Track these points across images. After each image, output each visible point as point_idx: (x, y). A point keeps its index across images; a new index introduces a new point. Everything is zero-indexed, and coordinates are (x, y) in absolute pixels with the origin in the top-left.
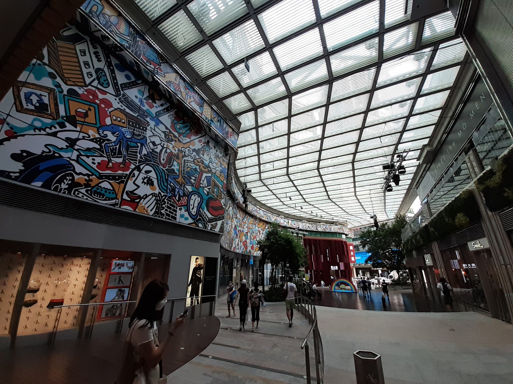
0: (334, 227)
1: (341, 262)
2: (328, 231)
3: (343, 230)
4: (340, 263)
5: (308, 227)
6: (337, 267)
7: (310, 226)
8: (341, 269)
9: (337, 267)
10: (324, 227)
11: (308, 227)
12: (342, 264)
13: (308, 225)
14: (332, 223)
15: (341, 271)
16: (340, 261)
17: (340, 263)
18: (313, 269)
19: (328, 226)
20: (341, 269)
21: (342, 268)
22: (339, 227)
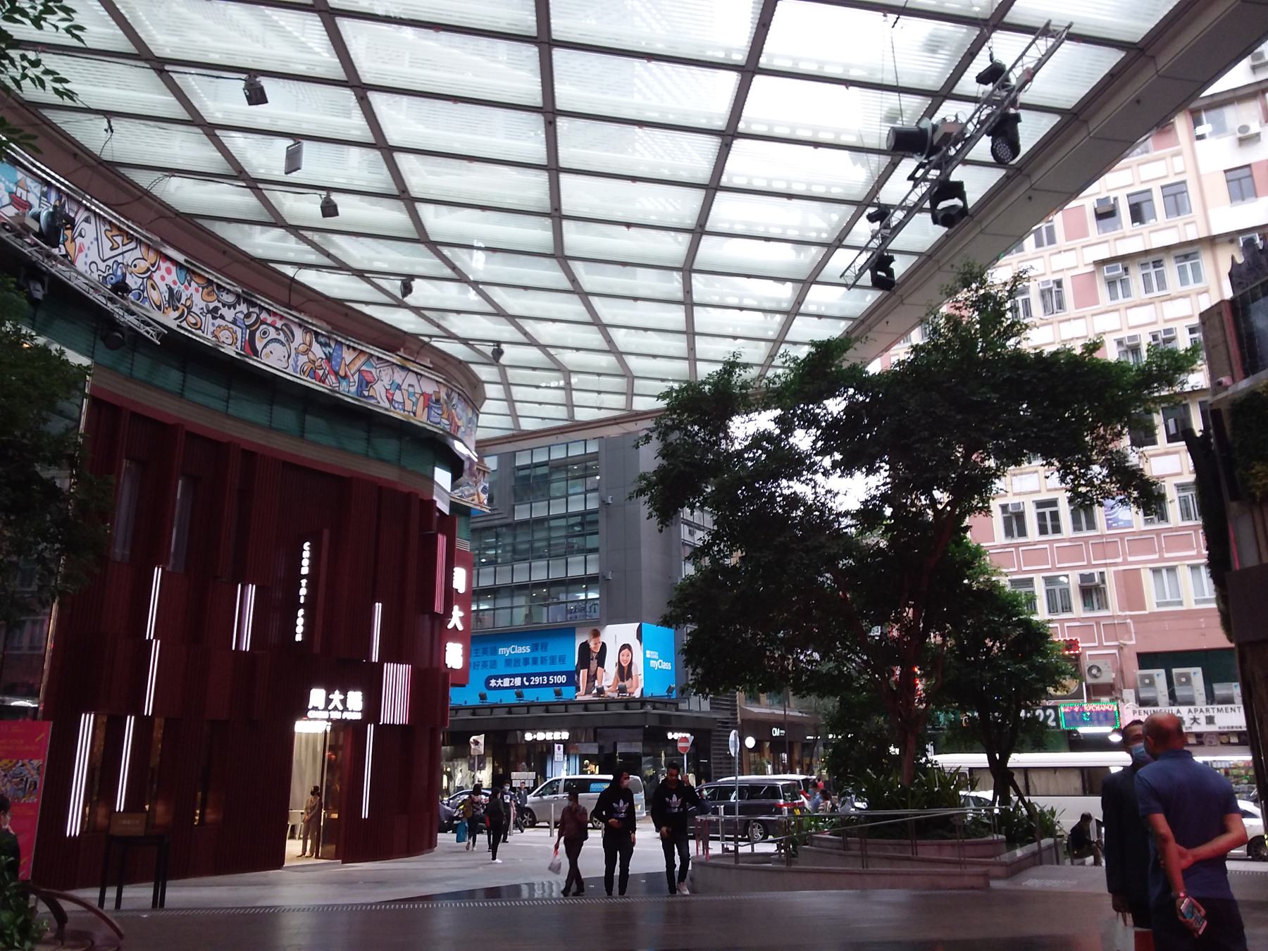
0: (399, 376)
1: (399, 661)
2: (348, 391)
3: (451, 418)
4: (389, 668)
5: (173, 297)
6: (356, 700)
7: (195, 295)
8: (386, 718)
9: (356, 700)
10: (318, 351)
11: (173, 297)
12: (396, 678)
13: (166, 277)
14: (391, 339)
15: (382, 731)
16: (392, 653)
17: (389, 668)
18: (137, 709)
19: (348, 356)
20: (386, 718)
21: (395, 710)
22: (429, 388)
